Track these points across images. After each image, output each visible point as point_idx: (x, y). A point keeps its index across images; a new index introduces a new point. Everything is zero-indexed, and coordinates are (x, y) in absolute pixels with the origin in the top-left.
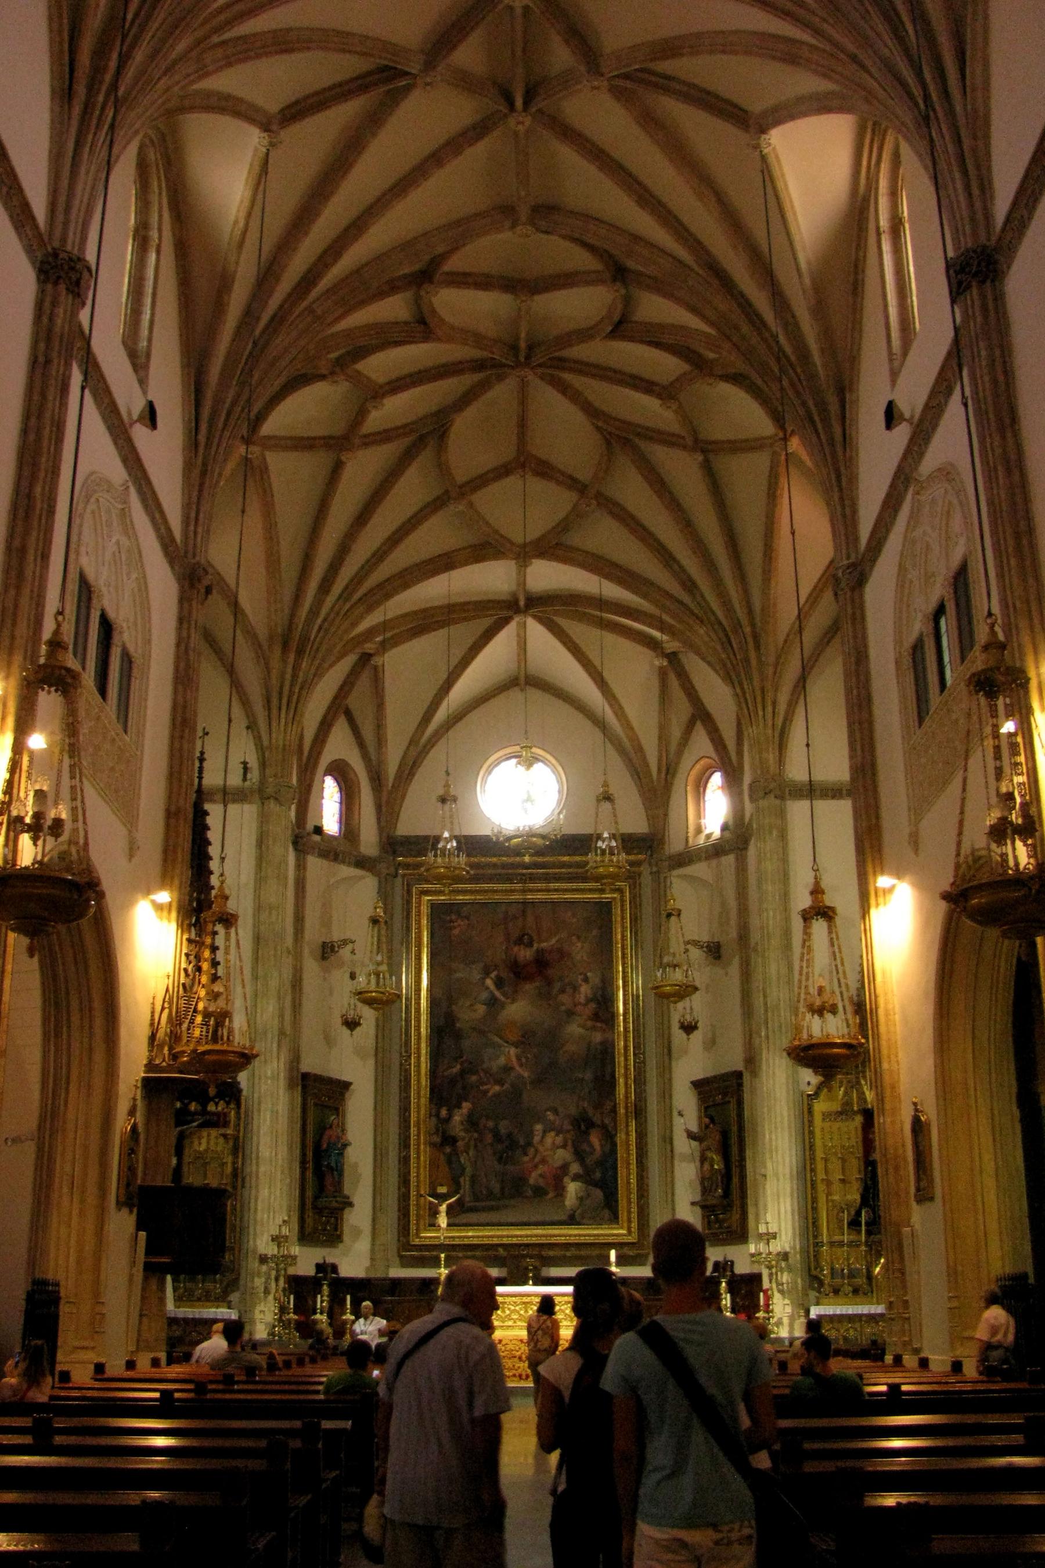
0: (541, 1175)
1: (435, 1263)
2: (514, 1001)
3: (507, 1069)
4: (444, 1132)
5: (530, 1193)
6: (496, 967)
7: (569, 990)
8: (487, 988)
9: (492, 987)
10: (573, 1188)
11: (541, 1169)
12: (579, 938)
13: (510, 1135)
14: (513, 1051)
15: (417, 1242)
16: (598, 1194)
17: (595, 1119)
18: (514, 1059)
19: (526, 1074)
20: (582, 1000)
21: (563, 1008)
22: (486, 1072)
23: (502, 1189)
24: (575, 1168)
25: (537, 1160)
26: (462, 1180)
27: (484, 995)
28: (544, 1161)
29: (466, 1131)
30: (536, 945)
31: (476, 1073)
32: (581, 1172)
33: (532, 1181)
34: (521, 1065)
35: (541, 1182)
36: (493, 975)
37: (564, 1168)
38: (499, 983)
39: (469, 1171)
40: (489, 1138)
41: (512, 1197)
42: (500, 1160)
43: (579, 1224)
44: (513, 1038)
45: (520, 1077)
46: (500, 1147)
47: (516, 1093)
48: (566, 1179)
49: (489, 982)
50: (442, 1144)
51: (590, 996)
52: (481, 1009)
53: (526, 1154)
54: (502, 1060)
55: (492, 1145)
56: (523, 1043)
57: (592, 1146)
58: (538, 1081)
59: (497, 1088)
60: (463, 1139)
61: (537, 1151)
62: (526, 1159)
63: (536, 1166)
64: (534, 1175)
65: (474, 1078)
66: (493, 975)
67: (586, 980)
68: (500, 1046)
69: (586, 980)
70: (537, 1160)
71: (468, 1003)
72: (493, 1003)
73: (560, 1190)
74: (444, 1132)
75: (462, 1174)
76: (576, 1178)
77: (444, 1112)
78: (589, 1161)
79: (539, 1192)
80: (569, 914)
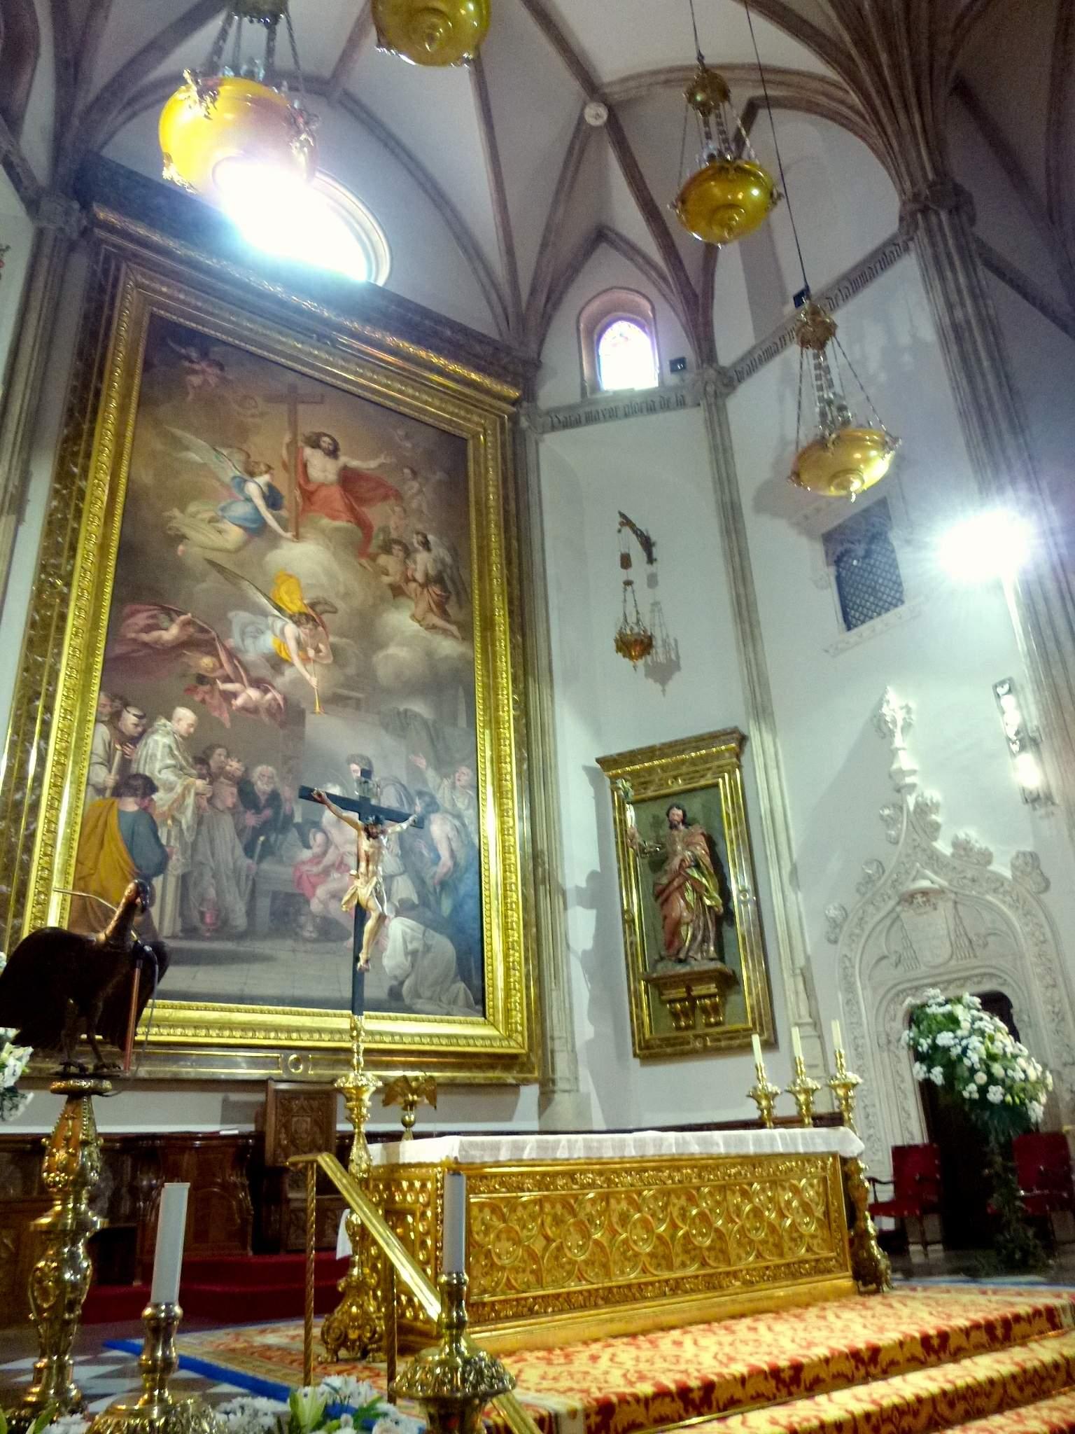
2: (298, 537)
3: (277, 663)
4: (126, 763)
5: (309, 931)
6: (269, 469)
7: (396, 549)
8: (249, 500)
9: (260, 503)
12: (415, 474)
13: (274, 797)
14: (291, 629)
17: (438, 796)
18: (292, 645)
19: (314, 681)
20: (419, 576)
21: (386, 580)
22: (231, 655)
23: (251, 912)
26: (157, 882)
27: (240, 510)
29: (179, 769)
30: (343, 459)
31: (213, 653)
32: (415, 899)
33: (315, 906)
34: (306, 660)
36: (263, 479)
38: (273, 498)
39: (176, 865)
40: (229, 795)
42: (249, 850)
43: (410, 1010)
44: (295, 606)
45: (300, 682)
46: (251, 819)
47: (290, 715)
49: (252, 489)
50: (118, 792)
51: (432, 572)
52: (234, 535)
53: (308, 847)
54: (269, 642)
55: (233, 811)
56: (309, 618)
57: (433, 849)
58: (333, 701)
59: (253, 694)
60: (171, 789)
61: (328, 842)
62: (306, 854)
63: (326, 872)
64: (321, 892)
65: (207, 662)
66: (263, 479)
67: (426, 545)
68: (265, 614)
69: (426, 545)
71: (207, 516)
72: (256, 529)
74: (126, 763)
75: (161, 868)
76: (404, 909)
77: (130, 719)
80: (401, 432)
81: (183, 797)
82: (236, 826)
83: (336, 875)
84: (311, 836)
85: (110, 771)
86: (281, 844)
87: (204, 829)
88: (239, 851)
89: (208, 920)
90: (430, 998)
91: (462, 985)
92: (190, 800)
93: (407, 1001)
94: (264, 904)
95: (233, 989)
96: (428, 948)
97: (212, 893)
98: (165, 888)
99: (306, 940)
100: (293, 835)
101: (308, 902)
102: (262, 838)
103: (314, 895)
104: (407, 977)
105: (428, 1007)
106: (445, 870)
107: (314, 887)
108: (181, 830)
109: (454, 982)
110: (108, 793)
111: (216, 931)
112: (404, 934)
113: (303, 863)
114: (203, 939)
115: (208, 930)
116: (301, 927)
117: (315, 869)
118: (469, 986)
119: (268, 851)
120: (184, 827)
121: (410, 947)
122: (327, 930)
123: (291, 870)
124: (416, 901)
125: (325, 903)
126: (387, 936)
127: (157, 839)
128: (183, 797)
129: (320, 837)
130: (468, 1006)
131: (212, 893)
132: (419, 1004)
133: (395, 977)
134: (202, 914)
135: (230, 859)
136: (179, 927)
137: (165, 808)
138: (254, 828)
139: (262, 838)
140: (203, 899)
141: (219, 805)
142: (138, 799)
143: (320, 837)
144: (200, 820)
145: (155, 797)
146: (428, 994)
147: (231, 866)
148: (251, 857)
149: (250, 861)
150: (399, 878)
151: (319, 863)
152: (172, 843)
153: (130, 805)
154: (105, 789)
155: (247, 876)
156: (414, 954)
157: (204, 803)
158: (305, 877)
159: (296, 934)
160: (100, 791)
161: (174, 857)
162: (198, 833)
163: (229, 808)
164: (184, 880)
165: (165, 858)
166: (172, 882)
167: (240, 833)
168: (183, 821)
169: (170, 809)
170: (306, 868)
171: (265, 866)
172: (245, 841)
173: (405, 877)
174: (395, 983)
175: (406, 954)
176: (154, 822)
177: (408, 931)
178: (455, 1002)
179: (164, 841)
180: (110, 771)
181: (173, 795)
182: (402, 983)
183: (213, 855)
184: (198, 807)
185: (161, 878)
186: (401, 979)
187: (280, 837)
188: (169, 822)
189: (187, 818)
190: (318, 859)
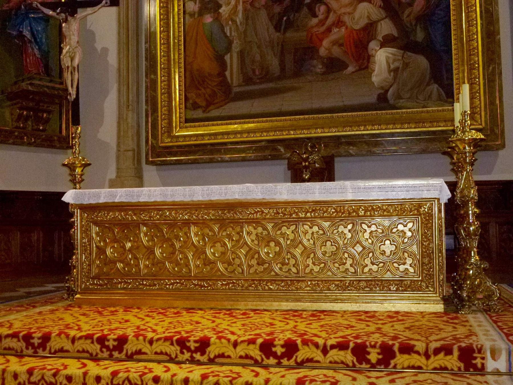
0: (335, 43)
1: (152, 161)
5: (319, 68)
10: (382, 57)
11: (337, 33)
15: (167, 142)
16: (422, 62)
23: (282, 64)
24: (386, 28)
25: (329, 22)
26: (227, 58)
28: (339, 23)
32: (395, 33)
33: (323, 52)
35: (336, 51)
37: (369, 30)
39: (236, 46)
41: (297, 74)
42: (277, 28)
43: (394, 107)
46: (277, 9)
48: (373, 45)
50: (201, 13)
53: (315, 16)
55: (266, 7)
61: (329, 10)
62: (315, 21)
63: (329, 30)
70: (329, 22)
73: (364, 61)
75: (229, 49)
76: (387, 42)
78: (408, 15)
79: (334, 66)
81: (236, 6)
82: (268, 15)
83: (336, 30)
84: (317, 9)
85: (196, 3)
86: (297, 19)
87: (250, 22)
88: (272, 29)
89: (257, 73)
90: (409, 98)
91: (436, 86)
92: (240, 8)
93: (391, 102)
94: (289, 59)
95: (275, 109)
96: (406, 65)
97: (258, 58)
98: (232, 60)
99: (317, 74)
100: (305, 10)
101: (318, 51)
102: (285, 18)
103: (321, 45)
104: (391, 86)
105: (409, 104)
106: (419, 8)
107: (321, 40)
108: (237, 25)
109: (428, 84)
110: (196, 16)
111: (262, 78)
112: (387, 58)
113: (312, 27)
114: (255, 84)
115: (258, 79)
116: (314, 67)
117: (322, 29)
118: (441, 85)
119: (290, 25)
120: (239, 23)
121: (392, 67)
122: (334, 66)
123: (305, 33)
124: (396, 34)
125: (329, 49)
126: (375, 63)
127: (225, 34)
128: (236, 6)
129: (323, 8)
130: (440, 99)
131: (258, 58)
132: (401, 103)
133: (382, 88)
134: (254, 71)
135: (267, 36)
136: (241, 80)
137: (227, 15)
138: (279, 13)
139: (285, 18)
140: (253, 61)
141: (257, 5)
142: (212, 14)
143: (323, 8)
144: (246, 18)
145: (220, 11)
146: (408, 95)
147: (268, 39)
148: (279, 31)
149: (278, 34)
150: (382, 22)
151: (324, 24)
152: (233, 34)
153: (208, 19)
154: (194, 14)
155: (278, 43)
156: (396, 70)
157: (249, 7)
158: (314, 37)
159: (311, 71)
160: (192, 15)
161: (235, 42)
162: (247, 25)
163: (263, 6)
164: (242, 54)
165: (230, 43)
166: (235, 55)
167: (271, 19)
168: (238, 20)
169: (229, 16)
170: (315, 30)
171: (288, 34)
172: (274, 23)
173: (387, 20)
174: (382, 91)
175: (390, 71)
176: (222, 25)
177: (390, 56)
178: (430, 97)
179: (228, 34)
180: (196, 3)
181: (230, 7)
182: (387, 91)
183: (256, 35)
184: (245, 10)
185: (229, 55)
186: (387, 88)
187: (296, 14)
188: (230, 23)
189: (239, 18)
190: (322, 23)
